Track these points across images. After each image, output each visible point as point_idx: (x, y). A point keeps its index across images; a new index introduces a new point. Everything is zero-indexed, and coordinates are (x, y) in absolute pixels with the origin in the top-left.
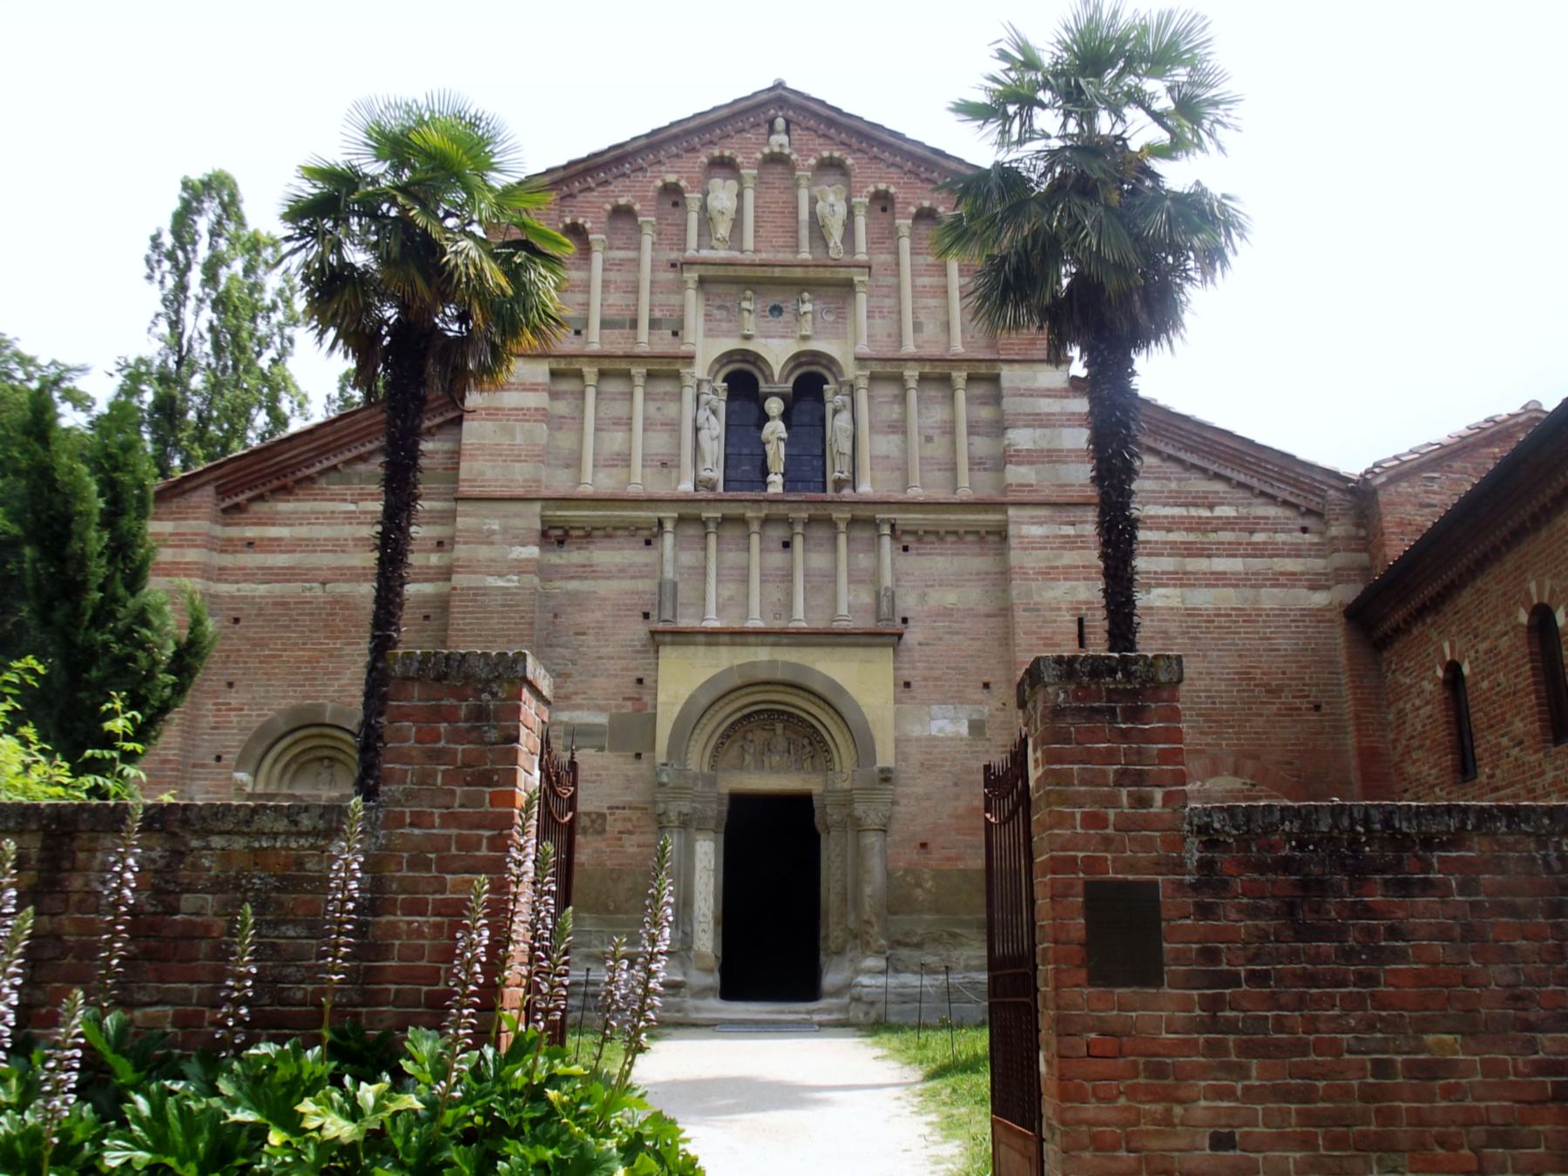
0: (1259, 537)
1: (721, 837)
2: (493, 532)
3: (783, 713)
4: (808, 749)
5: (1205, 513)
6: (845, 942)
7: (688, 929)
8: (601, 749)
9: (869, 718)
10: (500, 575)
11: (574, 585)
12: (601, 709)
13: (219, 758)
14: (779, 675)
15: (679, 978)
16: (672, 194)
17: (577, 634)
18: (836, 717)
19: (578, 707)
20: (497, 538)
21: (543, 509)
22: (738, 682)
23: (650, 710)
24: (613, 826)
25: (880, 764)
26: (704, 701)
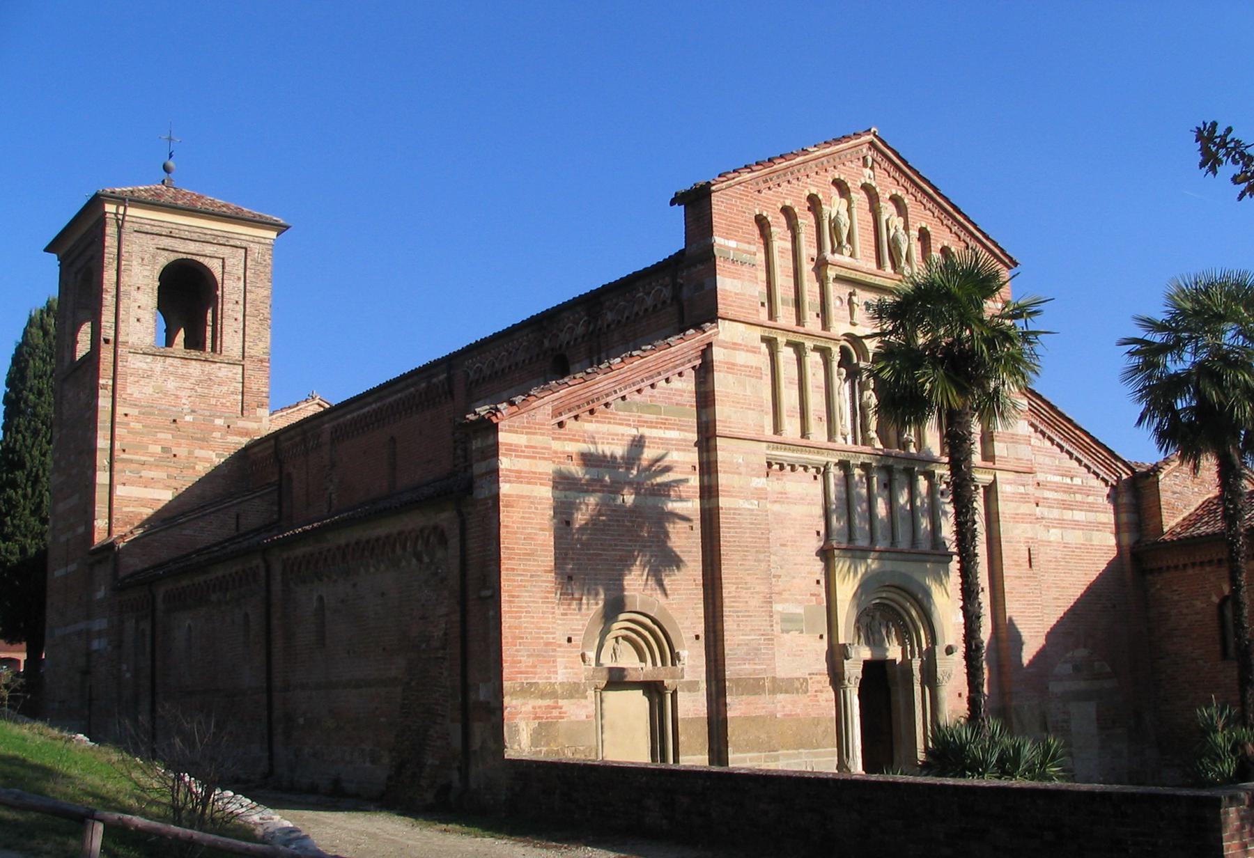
0: (1091, 499)
2: (739, 465)
5: (1068, 481)
8: (802, 632)
10: (746, 498)
11: (776, 507)
12: (800, 602)
13: (569, 640)
16: (814, 203)
17: (782, 545)
19: (787, 601)
20: (743, 469)
21: (768, 448)
24: (812, 687)
25: (948, 643)
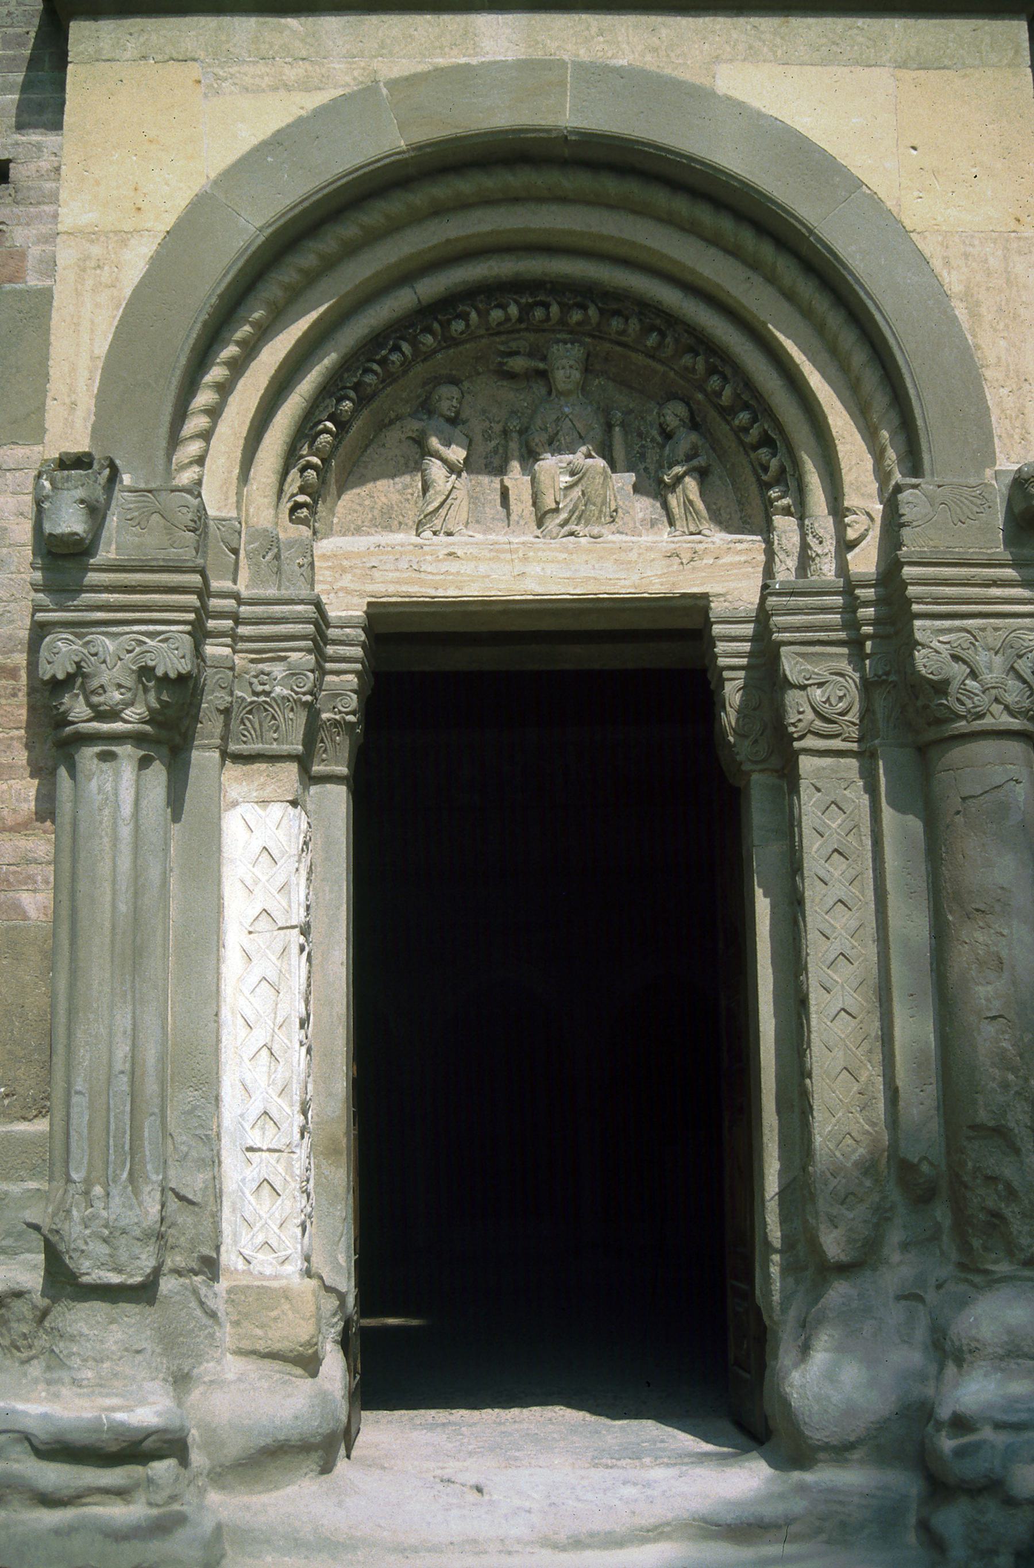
1: (336, 801)
3: (585, 293)
4: (686, 440)
6: (882, 1216)
7: (194, 1184)
9: (953, 281)
14: (568, 114)
15: (147, 1411)
18: (807, 289)
22: (389, 139)
23: (33, 281)
26: (252, 222)
